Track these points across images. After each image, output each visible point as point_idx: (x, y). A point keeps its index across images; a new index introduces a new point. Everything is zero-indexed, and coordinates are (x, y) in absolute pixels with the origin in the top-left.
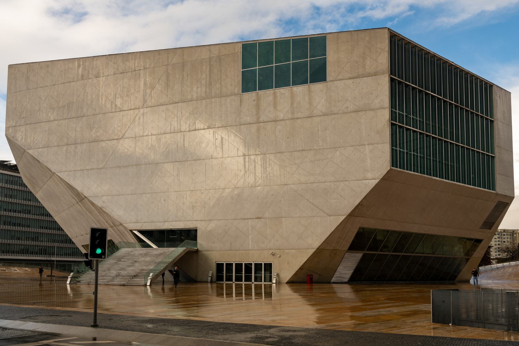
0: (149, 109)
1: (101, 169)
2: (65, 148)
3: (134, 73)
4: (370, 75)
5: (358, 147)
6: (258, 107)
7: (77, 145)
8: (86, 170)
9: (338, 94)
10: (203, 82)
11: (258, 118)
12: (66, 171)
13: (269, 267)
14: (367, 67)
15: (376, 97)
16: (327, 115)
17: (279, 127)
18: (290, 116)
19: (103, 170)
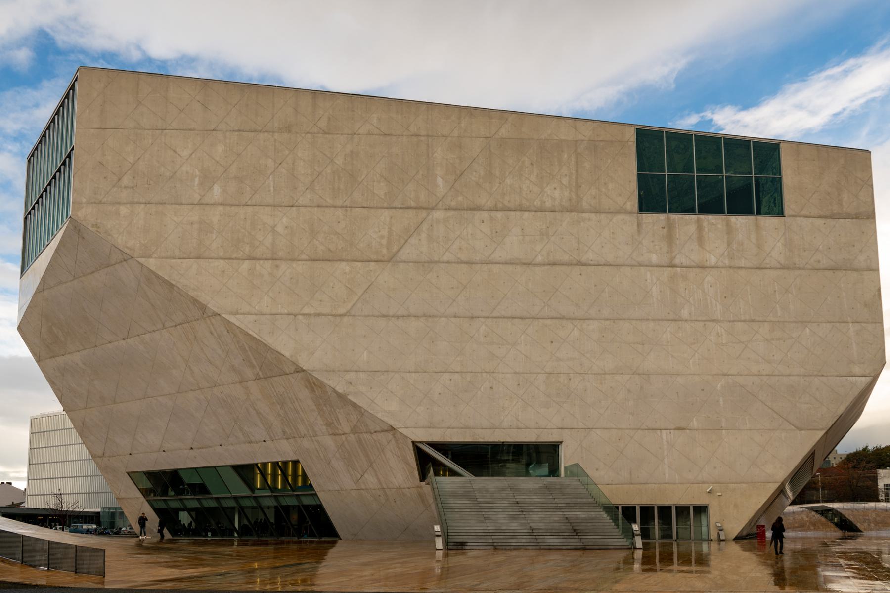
0: (452, 213)
1: (341, 316)
2: (246, 265)
3: (415, 139)
4: (848, 217)
5: (837, 324)
6: (670, 238)
7: (278, 262)
8: (303, 315)
9: (803, 238)
10: (565, 181)
11: (673, 258)
12: (249, 314)
13: (701, 510)
14: (844, 203)
15: (861, 251)
16: (788, 269)
17: (708, 278)
18: (727, 262)
19: (346, 319)
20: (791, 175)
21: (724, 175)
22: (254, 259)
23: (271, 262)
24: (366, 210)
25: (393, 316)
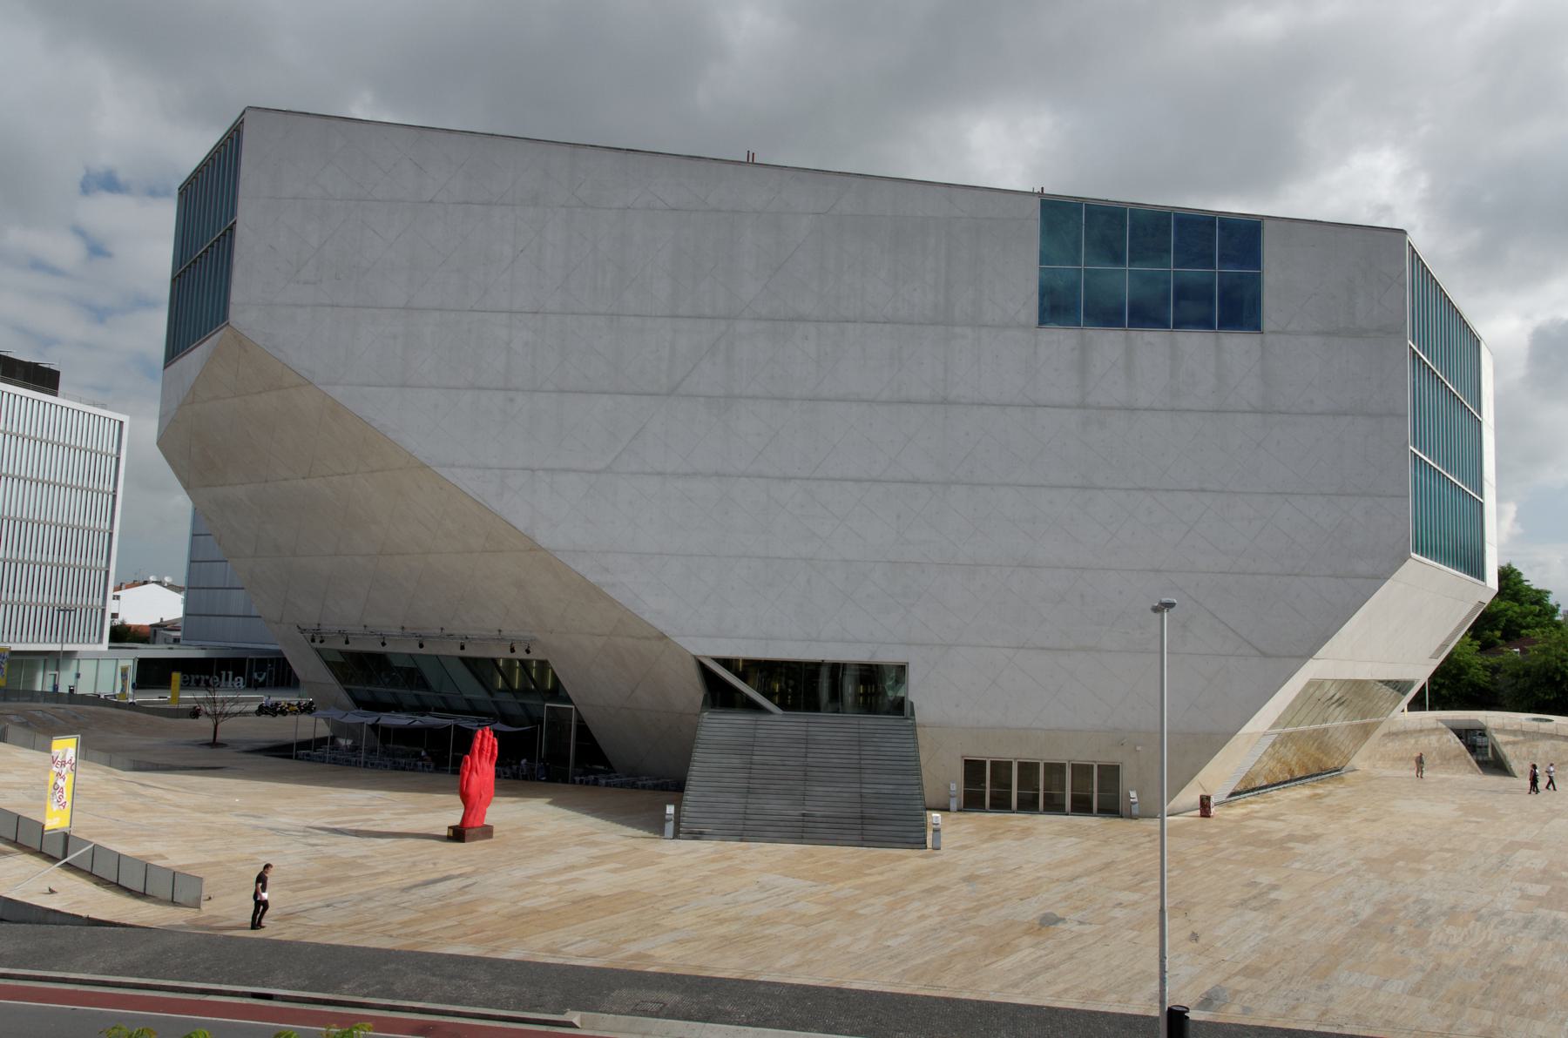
1: (597, 472)
8: (545, 470)
20: (1277, 273)
22: (479, 388)
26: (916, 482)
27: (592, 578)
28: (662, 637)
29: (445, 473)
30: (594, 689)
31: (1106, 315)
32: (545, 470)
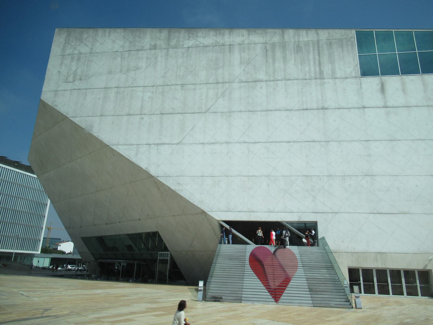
0: (243, 84)
1: (176, 144)
7: (143, 116)
8: (155, 144)
21: (417, 51)
23: (139, 116)
24: (193, 85)
25: (207, 143)
26: (314, 141)
27: (173, 188)
28: (203, 212)
29: (114, 147)
30: (178, 240)
31: (390, 69)
32: (155, 144)
